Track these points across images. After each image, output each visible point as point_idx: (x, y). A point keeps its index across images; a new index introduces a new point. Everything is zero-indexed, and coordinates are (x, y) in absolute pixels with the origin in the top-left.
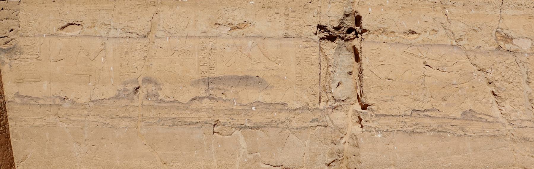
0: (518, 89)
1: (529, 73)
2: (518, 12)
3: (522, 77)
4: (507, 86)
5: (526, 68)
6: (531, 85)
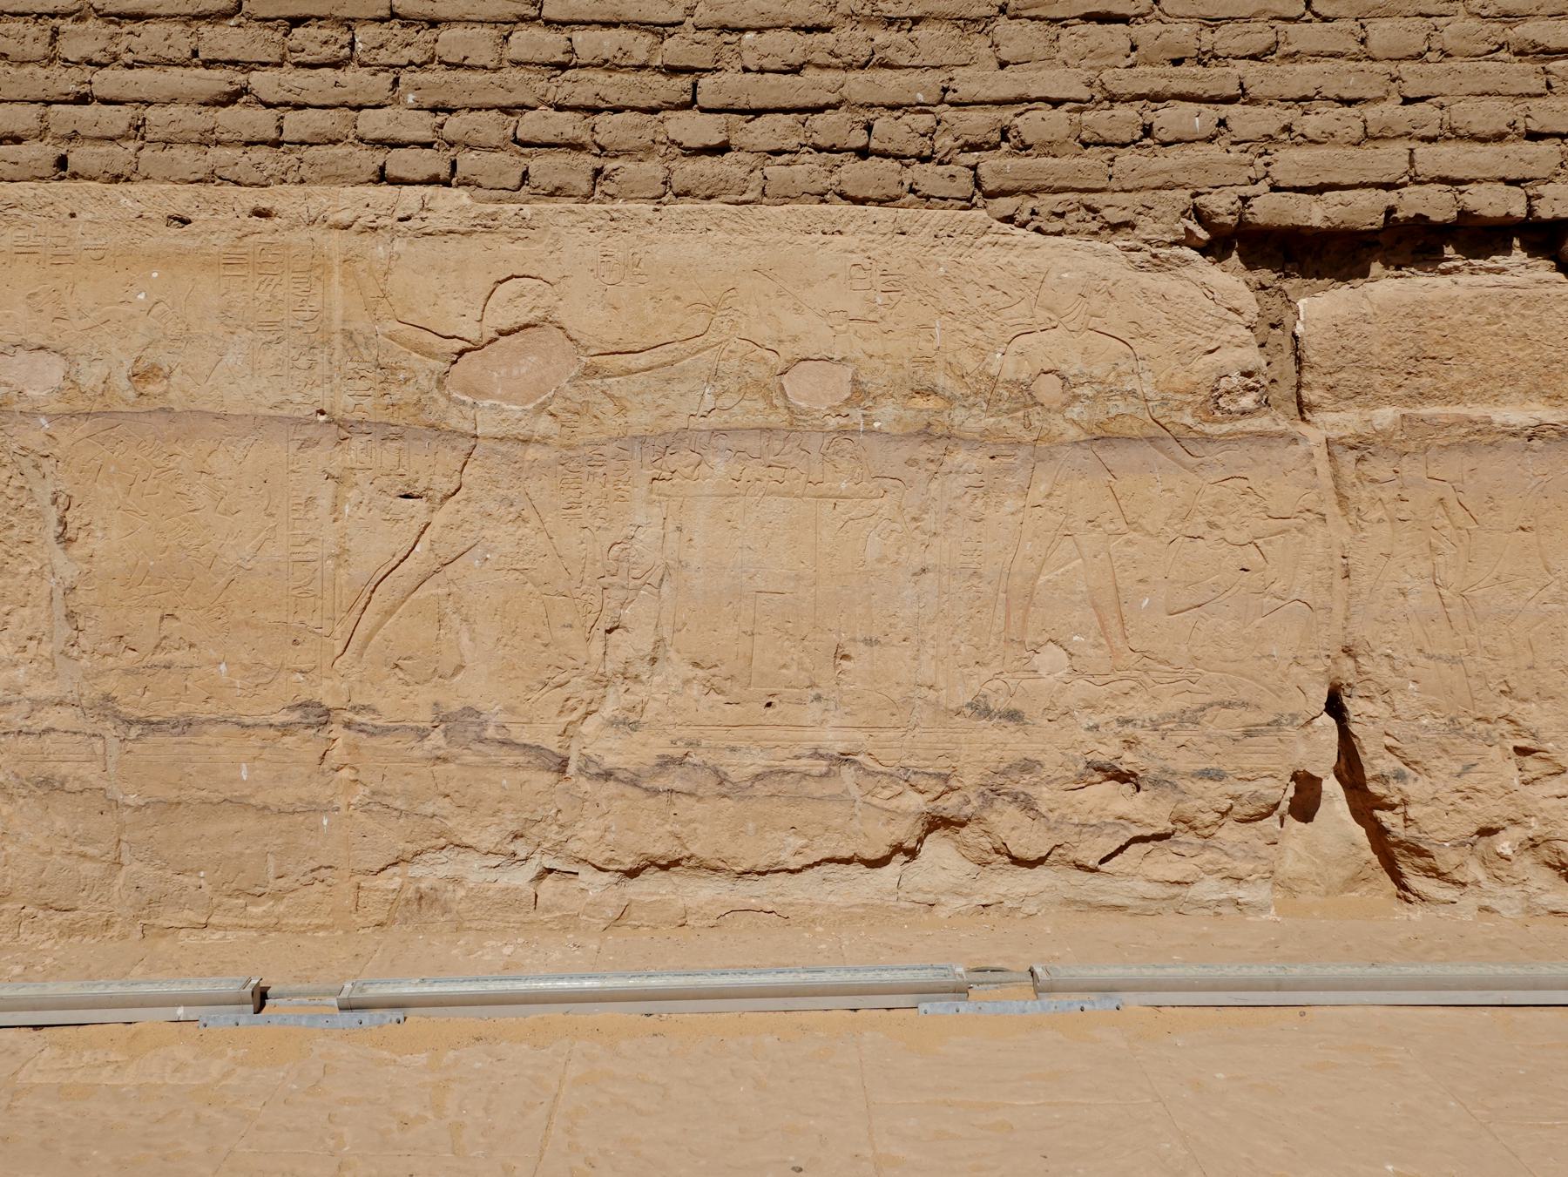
0: (27, 569)
1: (60, 500)
3: (37, 515)
5: (49, 480)
6: (75, 550)
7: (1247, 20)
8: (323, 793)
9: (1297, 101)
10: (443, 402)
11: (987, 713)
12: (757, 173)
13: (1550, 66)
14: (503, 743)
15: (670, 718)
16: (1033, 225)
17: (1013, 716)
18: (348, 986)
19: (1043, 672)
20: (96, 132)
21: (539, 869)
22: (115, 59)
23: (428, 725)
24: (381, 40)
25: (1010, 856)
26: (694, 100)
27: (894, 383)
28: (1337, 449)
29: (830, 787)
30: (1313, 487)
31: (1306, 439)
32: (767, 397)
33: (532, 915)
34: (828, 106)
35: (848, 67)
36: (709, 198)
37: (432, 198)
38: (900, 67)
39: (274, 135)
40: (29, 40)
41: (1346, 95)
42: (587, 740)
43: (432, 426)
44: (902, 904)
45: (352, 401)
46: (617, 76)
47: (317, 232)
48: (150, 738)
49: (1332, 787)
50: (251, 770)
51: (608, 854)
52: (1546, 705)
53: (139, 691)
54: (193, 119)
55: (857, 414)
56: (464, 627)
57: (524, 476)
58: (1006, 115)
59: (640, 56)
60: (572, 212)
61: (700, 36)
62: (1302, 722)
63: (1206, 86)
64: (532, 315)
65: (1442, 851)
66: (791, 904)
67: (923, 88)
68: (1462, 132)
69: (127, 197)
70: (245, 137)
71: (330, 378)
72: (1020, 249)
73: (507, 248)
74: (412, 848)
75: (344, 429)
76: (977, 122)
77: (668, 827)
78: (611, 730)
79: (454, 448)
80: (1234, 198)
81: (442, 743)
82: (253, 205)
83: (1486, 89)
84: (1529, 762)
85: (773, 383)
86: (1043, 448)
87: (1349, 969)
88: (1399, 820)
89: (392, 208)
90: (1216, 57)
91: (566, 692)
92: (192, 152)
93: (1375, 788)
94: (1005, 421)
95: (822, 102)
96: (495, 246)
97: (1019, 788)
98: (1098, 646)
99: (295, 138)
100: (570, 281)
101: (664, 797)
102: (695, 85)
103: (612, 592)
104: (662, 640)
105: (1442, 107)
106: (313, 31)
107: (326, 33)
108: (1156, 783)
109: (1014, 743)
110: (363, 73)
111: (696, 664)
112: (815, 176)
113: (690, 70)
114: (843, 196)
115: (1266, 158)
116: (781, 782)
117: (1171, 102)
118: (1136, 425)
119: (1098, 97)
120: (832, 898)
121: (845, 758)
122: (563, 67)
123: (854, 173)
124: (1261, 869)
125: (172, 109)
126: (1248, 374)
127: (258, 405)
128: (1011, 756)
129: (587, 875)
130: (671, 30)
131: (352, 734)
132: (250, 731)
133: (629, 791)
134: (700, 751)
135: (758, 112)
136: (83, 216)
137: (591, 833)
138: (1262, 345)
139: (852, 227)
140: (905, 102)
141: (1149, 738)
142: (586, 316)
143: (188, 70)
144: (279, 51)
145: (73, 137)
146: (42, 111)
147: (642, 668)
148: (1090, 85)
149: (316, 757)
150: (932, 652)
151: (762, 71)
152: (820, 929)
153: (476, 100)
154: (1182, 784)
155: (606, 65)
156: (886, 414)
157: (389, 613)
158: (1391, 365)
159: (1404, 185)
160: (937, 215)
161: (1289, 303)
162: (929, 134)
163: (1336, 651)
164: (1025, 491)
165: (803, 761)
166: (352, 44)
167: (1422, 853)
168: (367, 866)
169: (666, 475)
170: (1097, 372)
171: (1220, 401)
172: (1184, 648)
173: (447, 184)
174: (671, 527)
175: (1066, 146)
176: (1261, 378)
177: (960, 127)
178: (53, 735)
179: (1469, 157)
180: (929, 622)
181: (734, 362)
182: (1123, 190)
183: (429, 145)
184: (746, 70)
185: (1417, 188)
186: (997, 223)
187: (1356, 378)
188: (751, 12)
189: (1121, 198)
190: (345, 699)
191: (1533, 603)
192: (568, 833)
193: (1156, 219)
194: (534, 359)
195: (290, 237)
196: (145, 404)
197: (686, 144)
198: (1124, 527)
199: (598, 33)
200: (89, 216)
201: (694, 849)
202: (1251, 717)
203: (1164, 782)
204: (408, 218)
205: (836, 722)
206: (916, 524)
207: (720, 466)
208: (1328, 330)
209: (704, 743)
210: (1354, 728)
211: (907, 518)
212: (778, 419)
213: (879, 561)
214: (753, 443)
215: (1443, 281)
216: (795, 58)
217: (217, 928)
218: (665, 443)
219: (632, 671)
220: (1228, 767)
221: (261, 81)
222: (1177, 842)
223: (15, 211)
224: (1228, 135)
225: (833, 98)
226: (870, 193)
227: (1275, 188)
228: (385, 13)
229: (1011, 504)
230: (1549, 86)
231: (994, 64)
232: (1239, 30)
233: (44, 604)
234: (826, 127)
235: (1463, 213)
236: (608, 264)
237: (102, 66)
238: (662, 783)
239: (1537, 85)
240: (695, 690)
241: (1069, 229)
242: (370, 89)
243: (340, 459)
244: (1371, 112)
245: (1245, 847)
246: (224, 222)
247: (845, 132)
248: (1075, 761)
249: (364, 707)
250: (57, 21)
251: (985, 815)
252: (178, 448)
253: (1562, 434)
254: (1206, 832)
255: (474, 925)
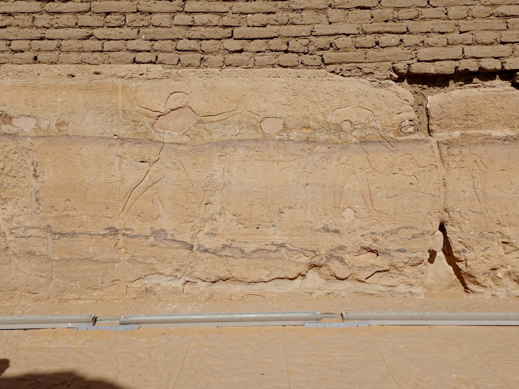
0: (24, 185)
1: (34, 164)
2: (19, 82)
3: (27, 168)
4: (9, 182)
5: (31, 157)
6: (39, 179)
7: (409, 8)
8: (115, 256)
9: (425, 33)
10: (153, 132)
11: (328, 231)
12: (252, 58)
13: (508, 21)
14: (173, 240)
15: (226, 232)
16: (341, 74)
17: (337, 231)
18: (123, 317)
19: (346, 217)
20: (46, 49)
21: (184, 281)
22: (52, 26)
23: (149, 235)
24: (134, 19)
25: (336, 277)
26: (232, 36)
27: (296, 125)
28: (440, 145)
29: (277, 255)
30: (433, 157)
31: (430, 141)
32: (256, 130)
33: (183, 296)
34: (275, 37)
35: (281, 25)
36: (237, 66)
37: (150, 68)
38: (297, 25)
39: (101, 49)
40: (26, 21)
41: (441, 31)
42: (199, 240)
43: (150, 139)
44: (301, 293)
45: (125, 132)
46: (208, 29)
47: (114, 79)
48: (62, 239)
49: (440, 254)
50: (93, 249)
51: (206, 276)
52: (512, 228)
53: (58, 224)
54: (76, 44)
55: (285, 135)
56: (160, 203)
57: (179, 155)
58: (332, 39)
59: (215, 22)
60: (194, 71)
61: (234, 16)
62: (431, 233)
63: (396, 29)
64: (181, 104)
65: (478, 276)
66: (265, 293)
67: (305, 31)
68: (479, 42)
69: (55, 69)
70: (92, 50)
71: (118, 124)
72: (337, 81)
73: (174, 83)
74: (144, 274)
75: (123, 140)
76: (322, 42)
77: (225, 267)
78: (207, 236)
79: (157, 146)
80: (406, 64)
81: (153, 240)
82: (94, 71)
83: (487, 28)
84: (507, 246)
85: (258, 125)
86: (345, 145)
87: (445, 313)
88: (464, 266)
89: (138, 71)
90: (399, 20)
91: (192, 224)
92: (75, 54)
93: (455, 255)
94: (333, 137)
95: (273, 36)
96: (170, 83)
97: (339, 255)
98: (364, 209)
99: (107, 50)
100: (193, 93)
101: (224, 258)
102: (232, 31)
103: (207, 192)
104: (223, 207)
105: (473, 34)
106: (113, 16)
107: (117, 17)
108: (383, 253)
109: (337, 241)
110: (129, 29)
111: (234, 215)
112: (271, 59)
113: (231, 27)
114: (280, 65)
115: (416, 52)
116: (262, 253)
117: (384, 34)
118: (375, 137)
119: (361, 33)
120: (278, 291)
121: (282, 245)
122: (191, 26)
123: (283, 58)
124: (419, 282)
125: (69, 41)
126: (411, 121)
127: (96, 133)
128: (336, 245)
129: (199, 283)
130: (225, 14)
131: (125, 237)
132: (93, 237)
133: (213, 256)
134: (236, 243)
135: (252, 39)
136: (41, 75)
137: (201, 269)
138: (416, 111)
139: (283, 75)
140: (299, 35)
141: (381, 239)
142: (199, 104)
143: (74, 29)
144: (103, 23)
145: (39, 50)
146: (30, 42)
147: (217, 217)
148: (358, 29)
149: (114, 245)
150: (310, 211)
151: (254, 26)
152: (275, 301)
153: (164, 37)
154: (392, 254)
155: (205, 25)
156: (294, 135)
157: (137, 199)
158: (458, 117)
159: (461, 59)
160: (310, 71)
161: (425, 98)
162: (307, 45)
163: (442, 210)
164: (339, 159)
165: (269, 246)
166: (125, 20)
167: (472, 276)
168: (130, 280)
169: (224, 154)
170: (362, 120)
171: (402, 129)
172: (392, 209)
173: (155, 63)
174: (226, 171)
175: (351, 49)
176: (415, 122)
177: (317, 43)
178: (32, 238)
179: (482, 50)
180: (309, 201)
181: (246, 118)
182: (370, 62)
183: (149, 51)
184: (248, 26)
185: (465, 60)
186: (329, 73)
187: (447, 121)
188: (250, 8)
189: (369, 65)
190: (123, 226)
191: (507, 194)
192: (194, 269)
193: (380, 71)
194: (182, 118)
195: (105, 80)
196: (61, 134)
197: (230, 50)
198: (372, 170)
199: (202, 15)
200: (44, 75)
201: (234, 274)
202: (414, 232)
203: (386, 253)
204: (142, 74)
205: (279, 234)
206: (304, 170)
207: (241, 151)
208: (437, 106)
209: (237, 240)
210: (448, 235)
211: (301, 168)
212: (260, 136)
213: (292, 182)
214: (251, 144)
215: (475, 90)
216: (264, 22)
217: (82, 299)
218: (225, 144)
219: (214, 217)
220: (407, 248)
221: (97, 33)
222: (391, 273)
223: (21, 74)
224: (403, 44)
225: (276, 35)
226: (288, 64)
227: (419, 61)
228: (135, 10)
229: (335, 163)
230: (508, 27)
231: (328, 23)
232: (406, 11)
233: (29, 196)
234: (274, 44)
235: (481, 68)
236: (206, 88)
237: (48, 28)
238: (223, 253)
239: (504, 27)
240: (234, 223)
241: (352, 75)
242: (131, 34)
243: (121, 150)
244: (449, 36)
245: (413, 274)
246: (85, 76)
247: (280, 45)
248: (357, 246)
249: (129, 229)
250: (34, 15)
251: (328, 264)
252: (71, 147)
253: (515, 139)
254: (400, 269)
255: (164, 299)
